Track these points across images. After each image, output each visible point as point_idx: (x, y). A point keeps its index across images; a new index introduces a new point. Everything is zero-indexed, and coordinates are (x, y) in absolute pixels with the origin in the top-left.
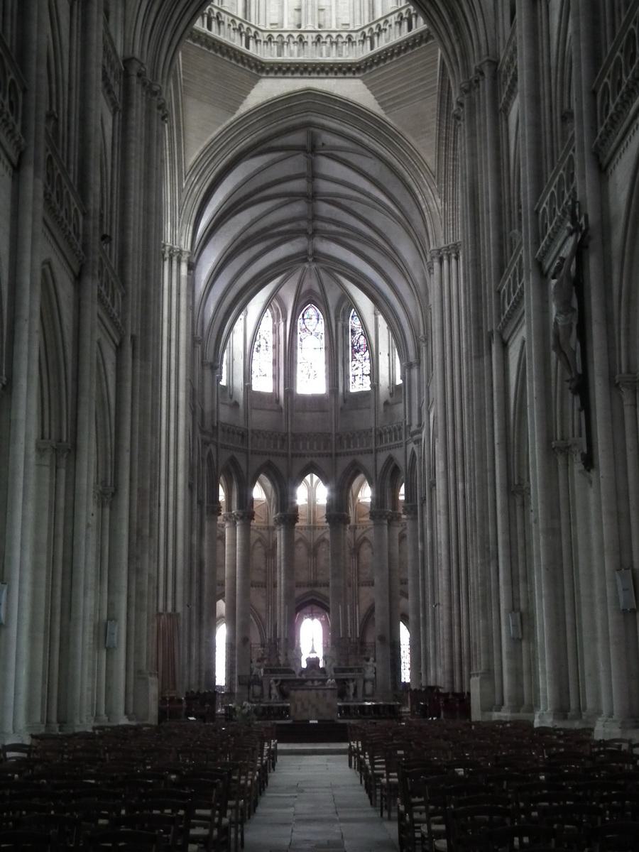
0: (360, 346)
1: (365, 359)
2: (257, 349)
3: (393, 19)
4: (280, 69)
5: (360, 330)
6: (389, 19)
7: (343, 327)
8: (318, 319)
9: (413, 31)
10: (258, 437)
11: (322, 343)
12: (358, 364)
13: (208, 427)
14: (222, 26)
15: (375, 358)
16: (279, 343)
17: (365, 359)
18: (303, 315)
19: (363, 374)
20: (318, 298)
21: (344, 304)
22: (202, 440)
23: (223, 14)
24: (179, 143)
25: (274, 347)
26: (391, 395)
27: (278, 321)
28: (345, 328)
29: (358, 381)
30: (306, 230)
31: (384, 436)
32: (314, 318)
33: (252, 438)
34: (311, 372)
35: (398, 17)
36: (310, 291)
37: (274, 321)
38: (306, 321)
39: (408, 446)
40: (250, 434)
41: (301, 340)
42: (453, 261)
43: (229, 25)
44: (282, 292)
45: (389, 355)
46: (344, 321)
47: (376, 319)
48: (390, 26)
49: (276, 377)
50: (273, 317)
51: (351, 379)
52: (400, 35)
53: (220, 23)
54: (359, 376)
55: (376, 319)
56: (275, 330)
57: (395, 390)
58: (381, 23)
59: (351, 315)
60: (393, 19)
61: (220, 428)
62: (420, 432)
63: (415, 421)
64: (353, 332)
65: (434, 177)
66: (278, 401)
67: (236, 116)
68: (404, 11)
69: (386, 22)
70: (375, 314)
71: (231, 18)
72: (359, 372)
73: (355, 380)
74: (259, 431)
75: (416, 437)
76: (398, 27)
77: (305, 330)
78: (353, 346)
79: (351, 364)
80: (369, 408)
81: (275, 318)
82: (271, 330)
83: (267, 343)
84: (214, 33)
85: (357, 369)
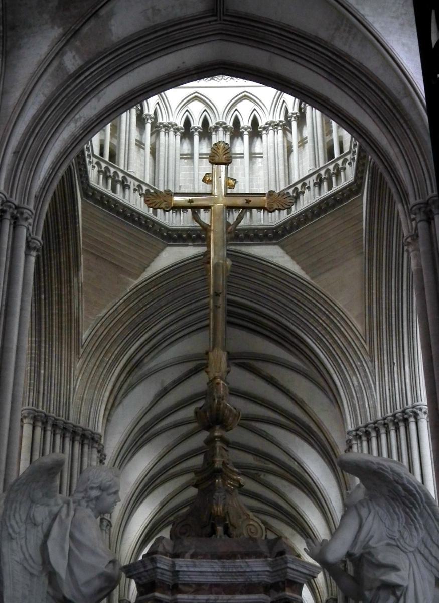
3: (311, 181)
4: (189, 236)
6: (307, 181)
9: (333, 189)
14: (127, 191)
23: (129, 179)
35: (317, 179)
43: (135, 190)
48: (309, 188)
52: (320, 195)
53: (125, 187)
58: (299, 186)
60: (311, 182)
65: (365, 342)
68: (323, 172)
69: (304, 184)
71: (137, 183)
76: (316, 189)
84: (119, 196)
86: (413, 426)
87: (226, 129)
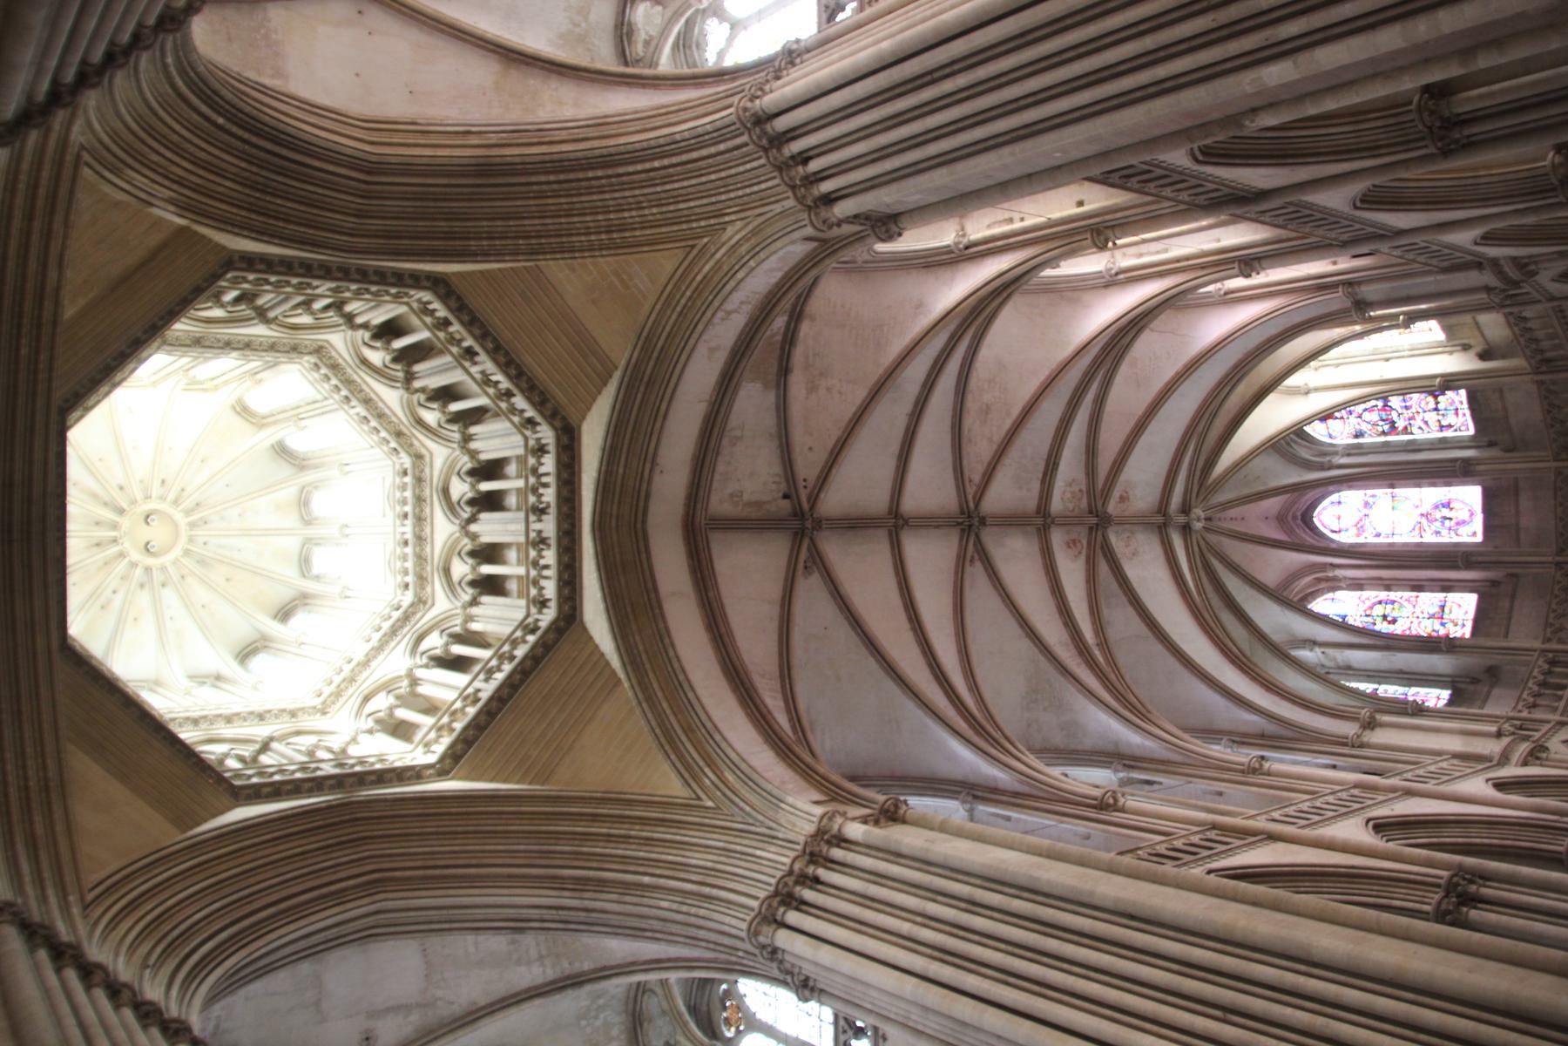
0: (1382, 420)
1: (1407, 408)
2: (1389, 622)
5: (1353, 420)
7: (1349, 455)
8: (1339, 503)
10: (1561, 629)
11: (1382, 495)
12: (1418, 422)
13: (1493, 747)
15: (1403, 385)
16: (1380, 579)
17: (1407, 408)
18: (1335, 532)
19: (1436, 409)
20: (1294, 503)
21: (1305, 454)
22: (1525, 764)
24: (630, 803)
25: (1388, 588)
26: (1466, 348)
27: (1335, 579)
28: (1350, 450)
29: (1451, 419)
30: (1091, 529)
31: (1549, 355)
32: (1336, 510)
33: (1560, 641)
34: (1438, 515)
36: (1281, 519)
37: (1340, 588)
38: (1343, 526)
39: (1557, 294)
40: (1547, 646)
41: (1378, 535)
42: (814, 166)
44: (1270, 577)
45: (1387, 360)
46: (1336, 453)
47: (1316, 390)
49: (1447, 587)
50: (1334, 589)
51: (1449, 434)
54: (1440, 418)
55: (1316, 390)
56: (1357, 585)
57: (1456, 341)
59: (1327, 440)
61: (1525, 714)
62: (1495, 263)
63: (1473, 278)
64: (1359, 435)
65: (693, 247)
66: (1494, 583)
67: (621, 674)
70: (1307, 393)
72: (1434, 426)
73: (1450, 426)
74: (1547, 624)
75: (1513, 274)
77: (1360, 529)
78: (1384, 433)
79: (1418, 436)
80: (1501, 391)
81: (1334, 585)
82: (1358, 593)
83: (1380, 602)
85: (1426, 423)
86: (781, 124)
87: (473, 519)
